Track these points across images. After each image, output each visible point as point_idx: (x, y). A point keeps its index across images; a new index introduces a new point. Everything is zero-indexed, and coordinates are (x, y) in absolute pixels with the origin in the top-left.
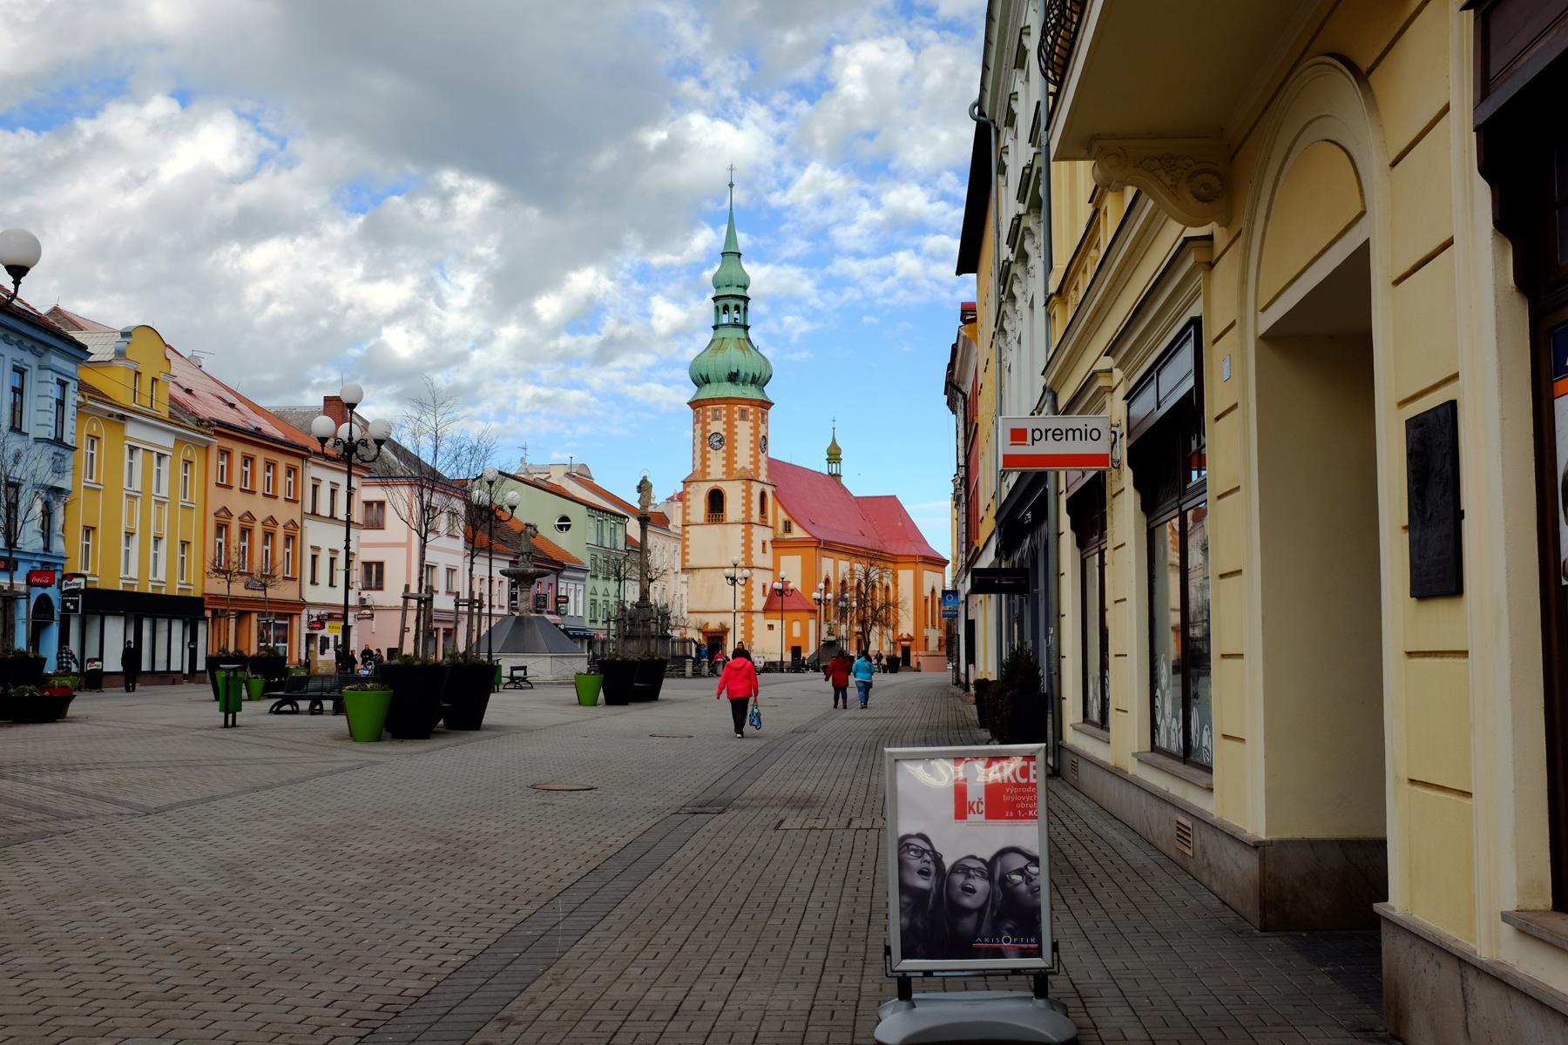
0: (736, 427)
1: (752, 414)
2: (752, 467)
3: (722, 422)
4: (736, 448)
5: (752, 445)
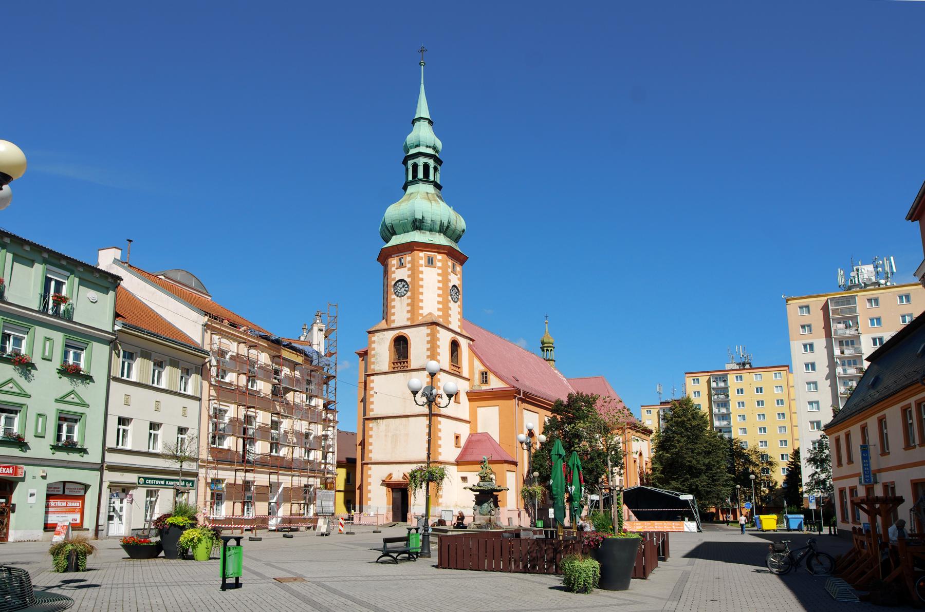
0: (422, 272)
1: (439, 261)
2: (440, 313)
3: (406, 269)
4: (422, 294)
5: (440, 292)
